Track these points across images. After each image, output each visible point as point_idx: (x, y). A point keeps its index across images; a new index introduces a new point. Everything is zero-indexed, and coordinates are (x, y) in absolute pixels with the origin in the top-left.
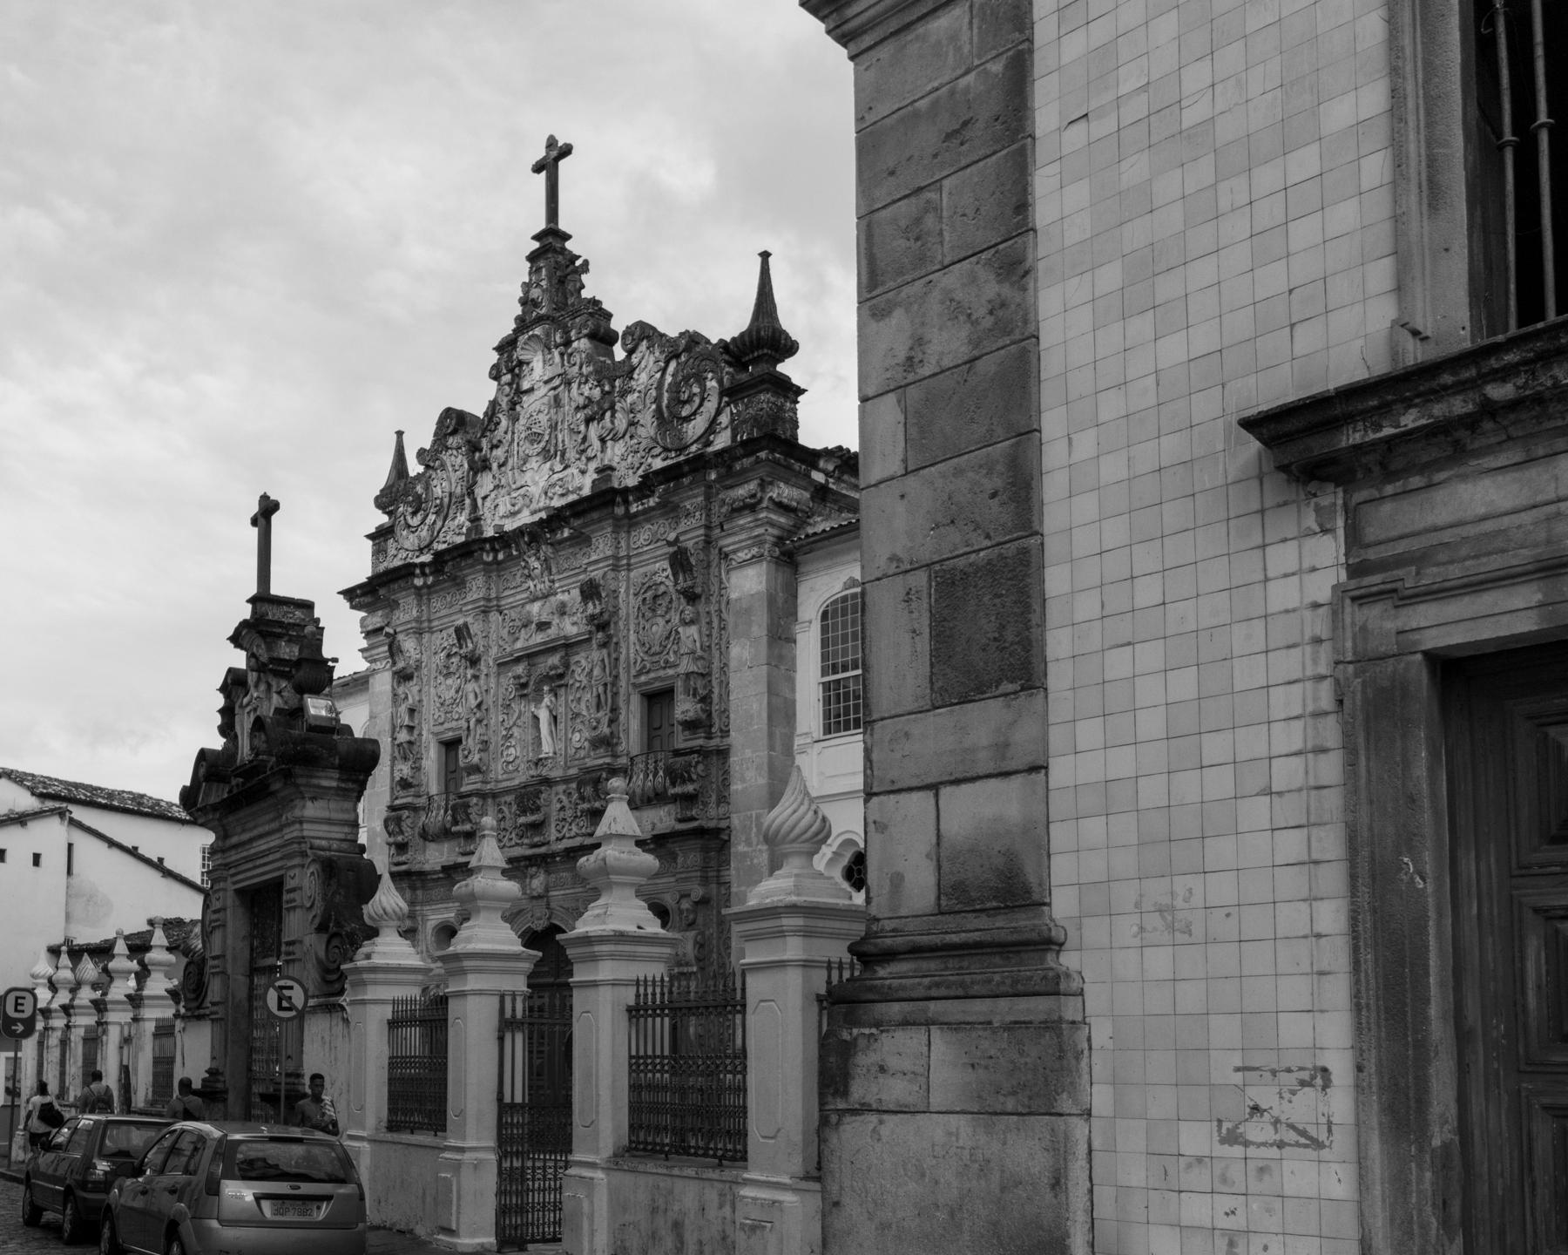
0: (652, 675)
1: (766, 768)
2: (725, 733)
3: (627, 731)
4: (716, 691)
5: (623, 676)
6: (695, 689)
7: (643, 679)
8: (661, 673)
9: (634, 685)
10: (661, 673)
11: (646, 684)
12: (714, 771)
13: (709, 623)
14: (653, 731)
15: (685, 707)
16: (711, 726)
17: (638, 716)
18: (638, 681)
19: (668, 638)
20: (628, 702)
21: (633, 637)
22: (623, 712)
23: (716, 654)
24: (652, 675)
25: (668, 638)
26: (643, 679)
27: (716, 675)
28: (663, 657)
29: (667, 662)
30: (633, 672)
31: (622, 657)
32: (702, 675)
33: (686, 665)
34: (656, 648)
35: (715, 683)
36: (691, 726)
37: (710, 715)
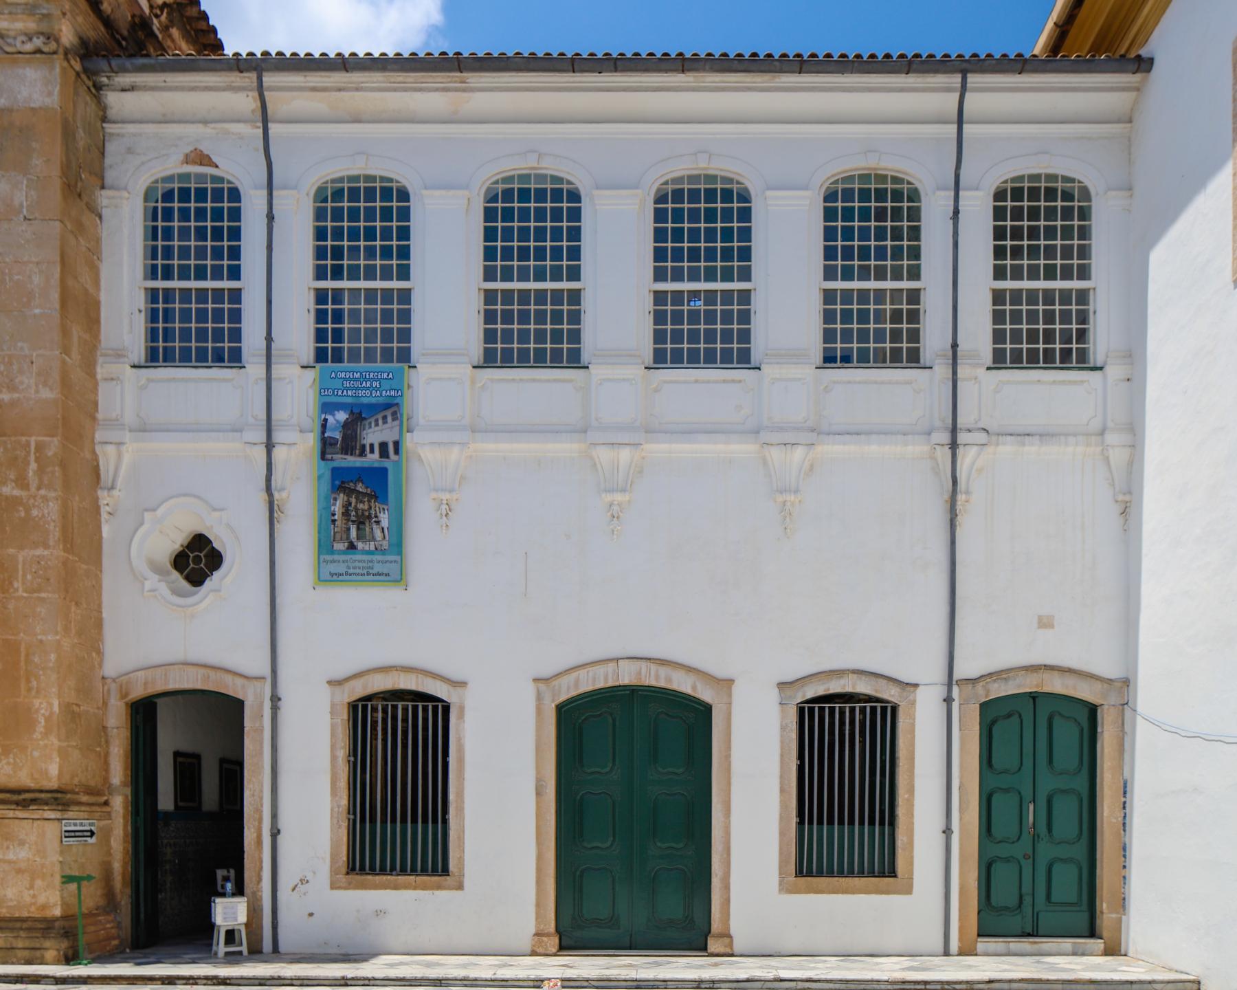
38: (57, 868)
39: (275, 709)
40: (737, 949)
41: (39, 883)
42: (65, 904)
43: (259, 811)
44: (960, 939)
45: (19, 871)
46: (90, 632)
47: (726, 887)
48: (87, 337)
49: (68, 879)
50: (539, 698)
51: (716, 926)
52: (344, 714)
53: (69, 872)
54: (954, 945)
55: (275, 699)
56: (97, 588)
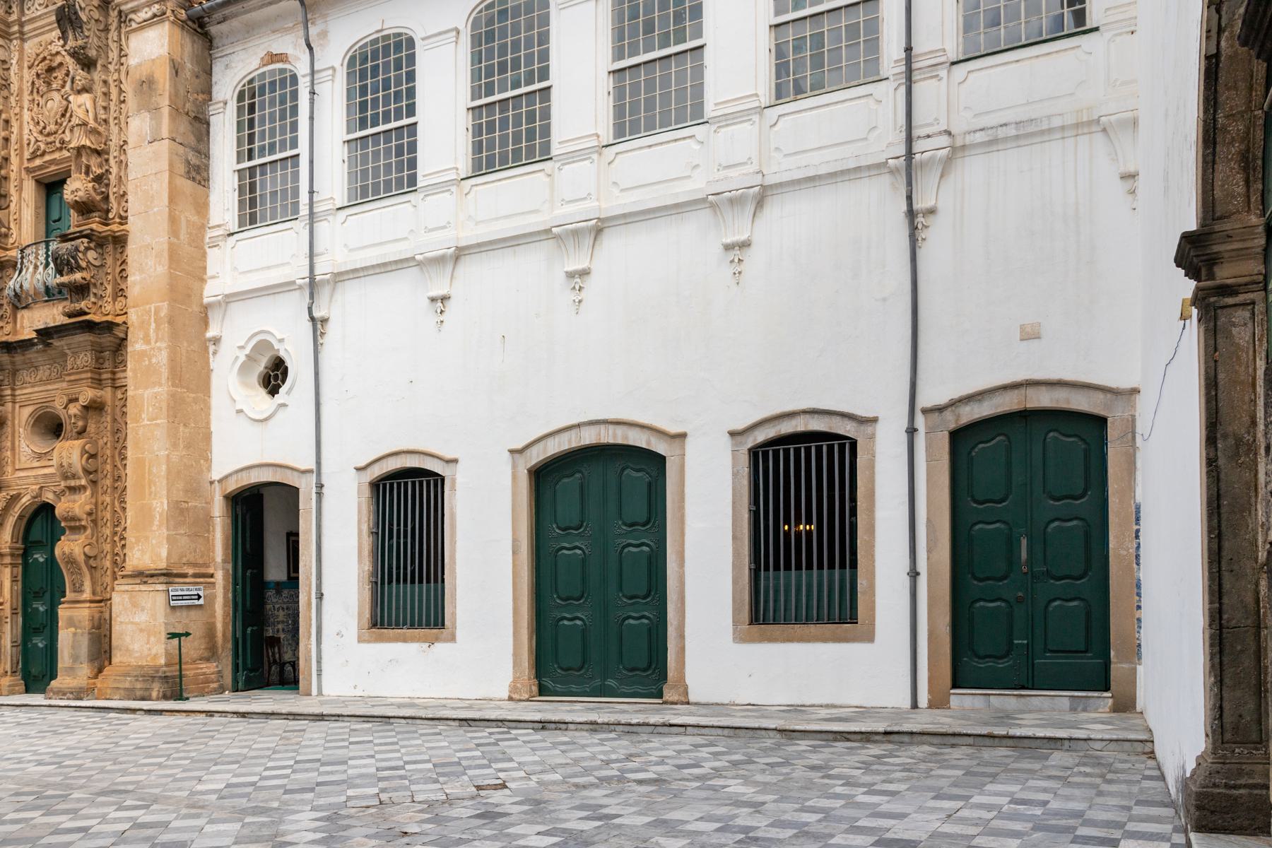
0: (47, 158)
1: (166, 254)
2: (123, 220)
3: (18, 221)
4: (114, 170)
5: (14, 160)
6: (88, 167)
7: (38, 162)
8: (57, 155)
9: (28, 170)
10: (57, 155)
11: (40, 168)
12: (109, 261)
13: (106, 94)
14: (50, 224)
15: (77, 188)
16: (108, 211)
17: (32, 204)
18: (31, 165)
19: (63, 115)
20: (20, 189)
21: (27, 116)
22: (14, 198)
23: (114, 129)
24: (47, 158)
25: (63, 115)
26: (38, 162)
27: (114, 153)
28: (58, 137)
29: (62, 142)
30: (27, 155)
31: (13, 138)
32: (98, 153)
33: (79, 139)
34: (52, 127)
35: (112, 162)
36: (85, 208)
37: (106, 198)
38: (163, 628)
39: (319, 494)
40: (692, 698)
41: (152, 639)
42: (167, 653)
43: (309, 578)
44: (930, 692)
45: (141, 630)
46: (198, 442)
47: (682, 636)
48: (195, 218)
49: (173, 636)
50: (514, 466)
51: (671, 674)
52: (367, 492)
53: (173, 631)
54: (923, 699)
55: (320, 486)
56: (206, 409)
